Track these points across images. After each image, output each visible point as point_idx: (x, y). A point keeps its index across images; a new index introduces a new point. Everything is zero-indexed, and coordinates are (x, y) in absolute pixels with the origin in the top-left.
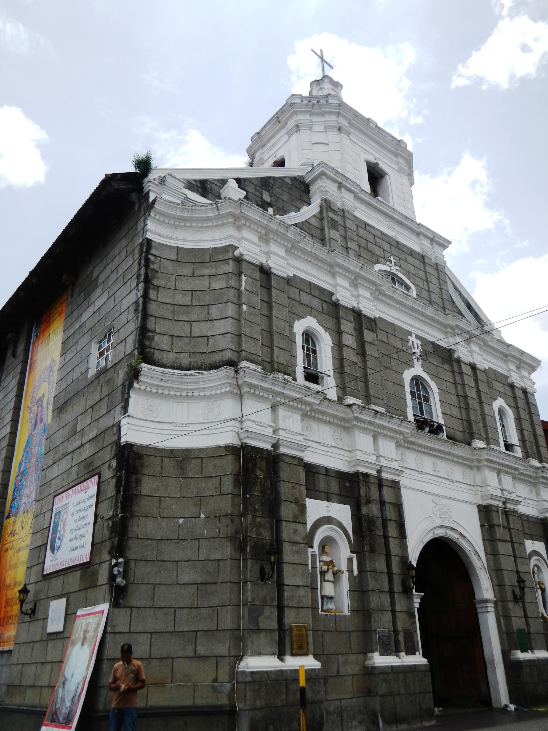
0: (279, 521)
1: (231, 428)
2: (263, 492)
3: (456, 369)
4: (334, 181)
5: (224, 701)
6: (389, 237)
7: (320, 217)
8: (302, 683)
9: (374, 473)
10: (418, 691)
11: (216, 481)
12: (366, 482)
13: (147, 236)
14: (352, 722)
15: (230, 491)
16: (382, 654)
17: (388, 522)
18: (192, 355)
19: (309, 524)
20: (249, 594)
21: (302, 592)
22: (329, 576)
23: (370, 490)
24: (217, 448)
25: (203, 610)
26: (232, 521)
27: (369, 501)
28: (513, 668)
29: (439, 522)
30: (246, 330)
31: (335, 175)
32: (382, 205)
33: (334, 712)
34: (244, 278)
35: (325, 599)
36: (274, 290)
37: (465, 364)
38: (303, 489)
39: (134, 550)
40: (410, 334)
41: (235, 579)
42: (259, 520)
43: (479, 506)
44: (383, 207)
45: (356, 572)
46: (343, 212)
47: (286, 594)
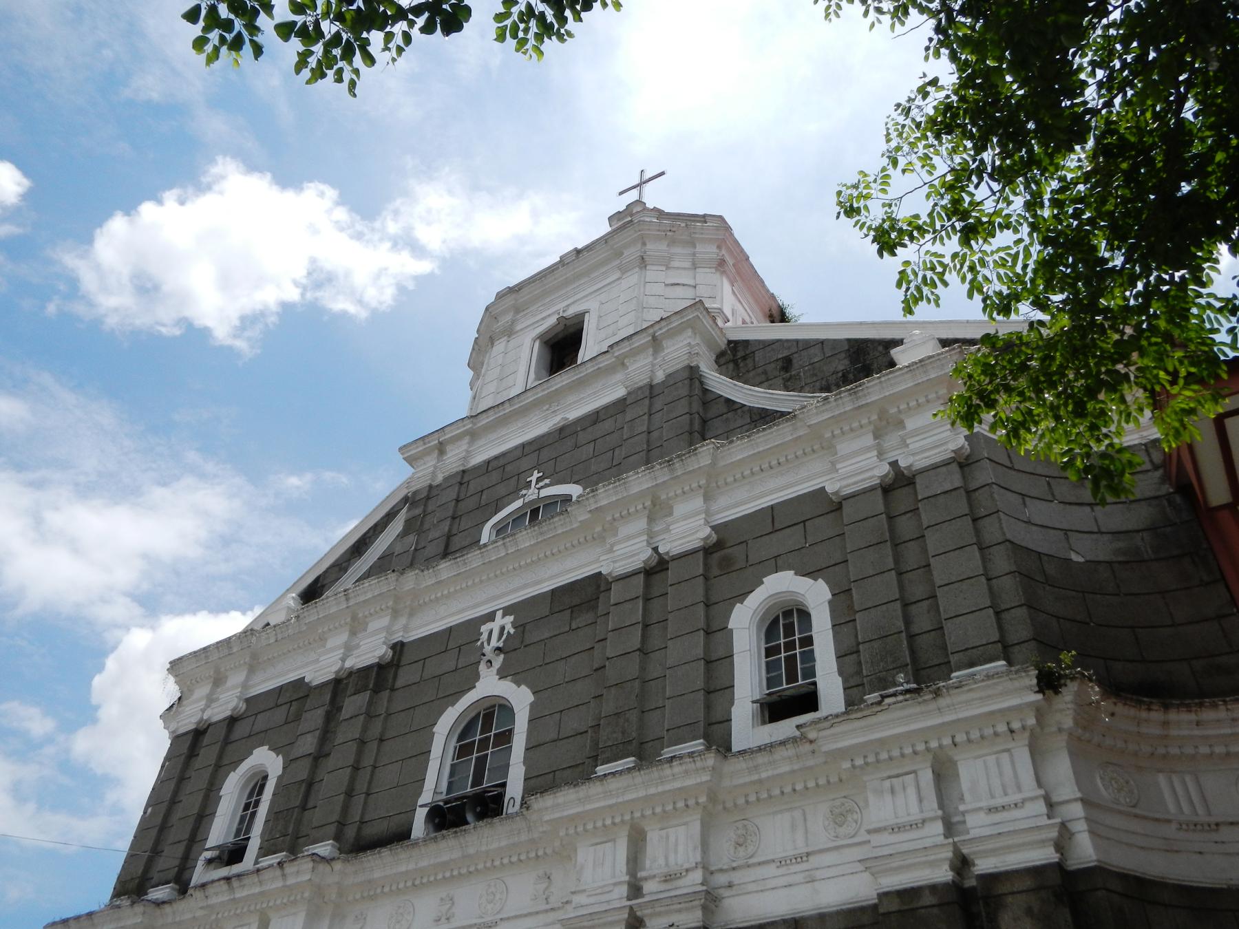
6: (543, 436)
40: (490, 617)
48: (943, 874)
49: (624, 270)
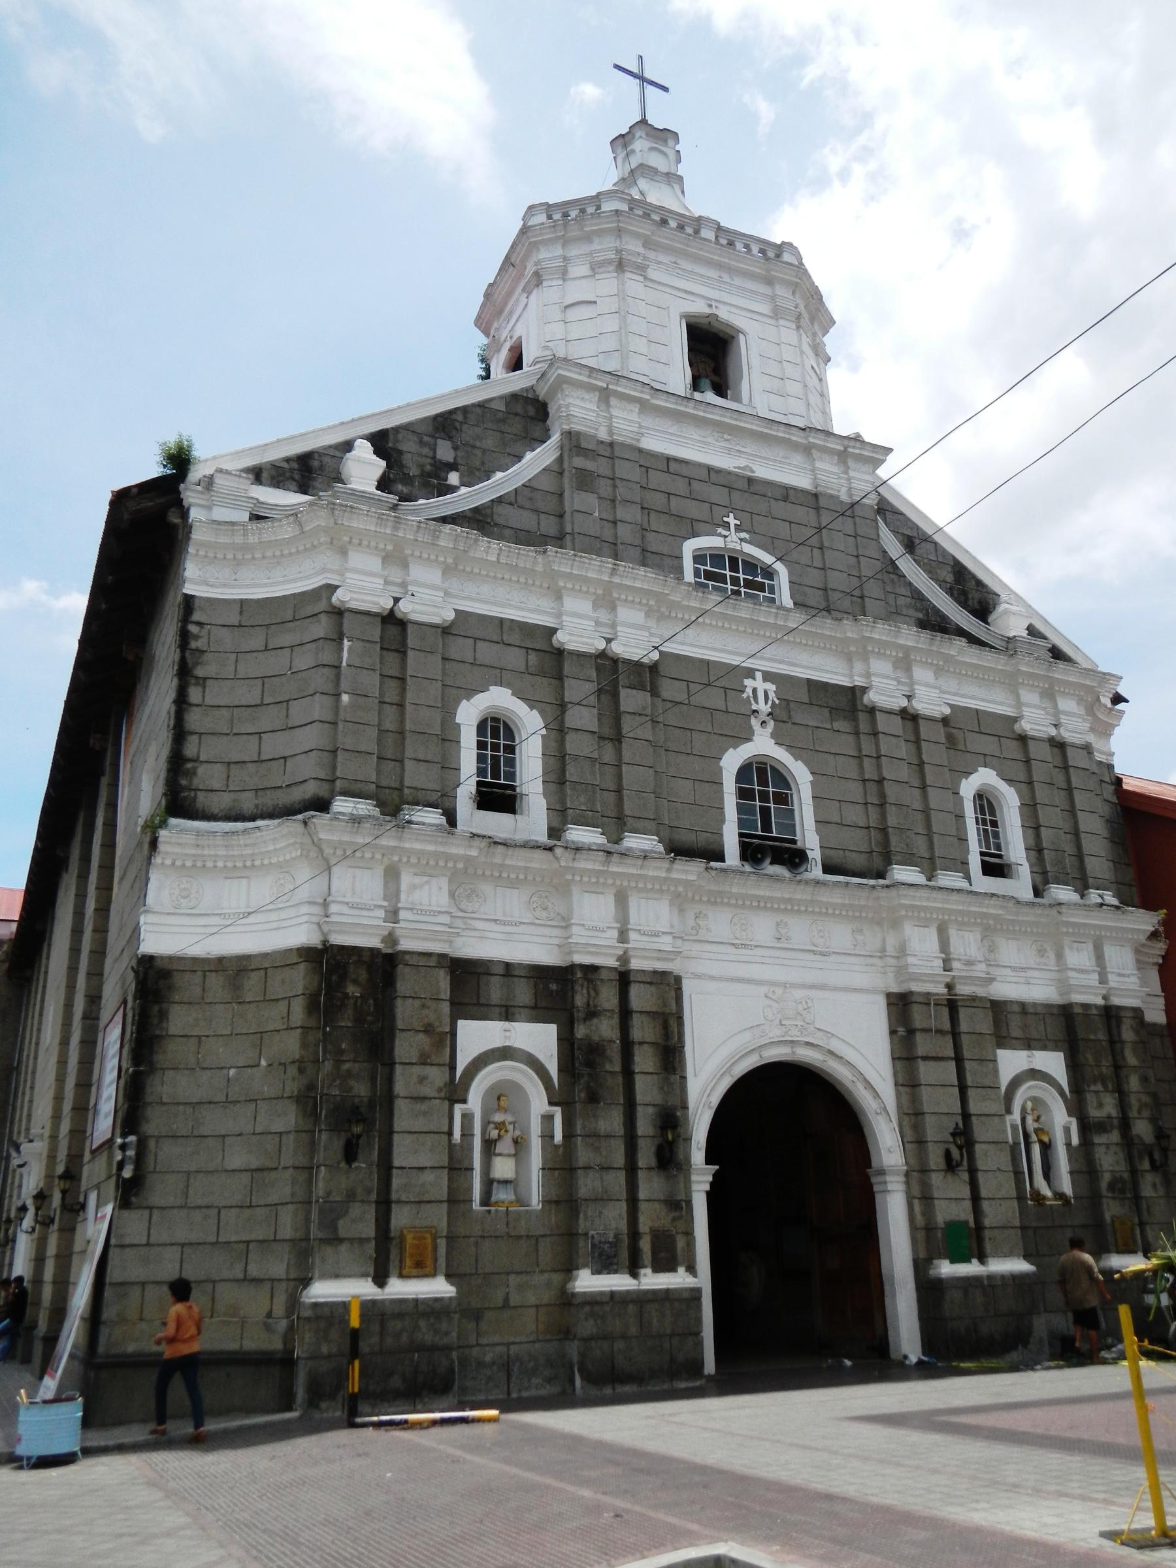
0: (391, 1064)
1: (305, 918)
2: (359, 1019)
3: (864, 726)
4: (590, 388)
5: (277, 1345)
6: (730, 473)
7: (557, 470)
8: (355, 1322)
9: (612, 962)
10: (668, 1331)
11: (283, 1006)
12: (590, 981)
13: (185, 591)
14: (529, 1380)
15: (299, 1024)
16: (596, 1272)
17: (636, 1047)
18: (260, 793)
19: (462, 1062)
20: (321, 1184)
21: (429, 1177)
22: (505, 1146)
23: (597, 993)
24: (288, 951)
25: (258, 1211)
26: (301, 1071)
27: (592, 1013)
28: (930, 1291)
29: (776, 1033)
30: (346, 740)
31: (589, 377)
32: (710, 409)
33: (494, 1363)
34: (346, 644)
35: (495, 1184)
36: (410, 653)
37: (889, 712)
38: (446, 1008)
39: (155, 1123)
40: (750, 673)
41: (303, 1161)
42: (346, 1066)
43: (889, 995)
44: (713, 413)
45: (558, 1137)
46: (611, 450)
47: (396, 1182)
48: (1099, 1001)
49: (777, 313)
